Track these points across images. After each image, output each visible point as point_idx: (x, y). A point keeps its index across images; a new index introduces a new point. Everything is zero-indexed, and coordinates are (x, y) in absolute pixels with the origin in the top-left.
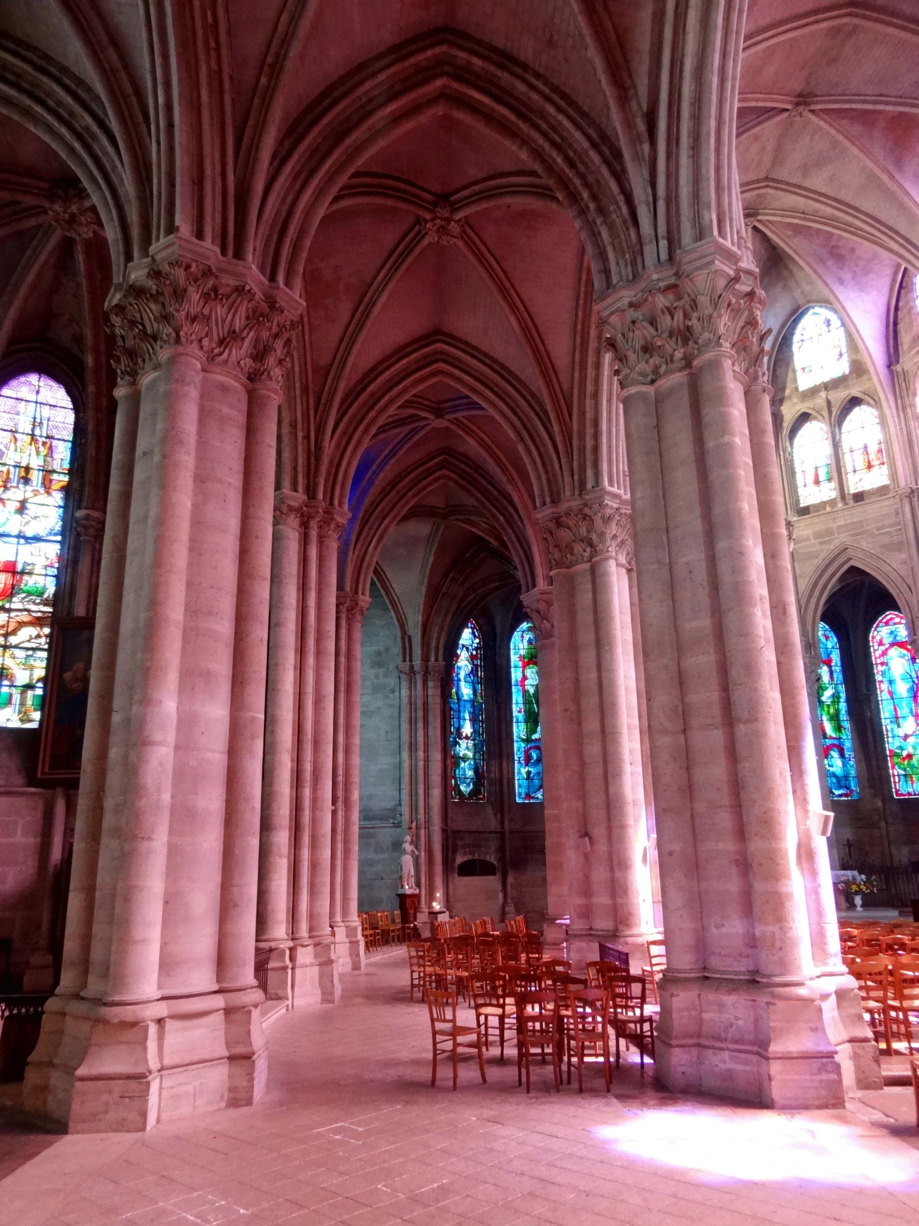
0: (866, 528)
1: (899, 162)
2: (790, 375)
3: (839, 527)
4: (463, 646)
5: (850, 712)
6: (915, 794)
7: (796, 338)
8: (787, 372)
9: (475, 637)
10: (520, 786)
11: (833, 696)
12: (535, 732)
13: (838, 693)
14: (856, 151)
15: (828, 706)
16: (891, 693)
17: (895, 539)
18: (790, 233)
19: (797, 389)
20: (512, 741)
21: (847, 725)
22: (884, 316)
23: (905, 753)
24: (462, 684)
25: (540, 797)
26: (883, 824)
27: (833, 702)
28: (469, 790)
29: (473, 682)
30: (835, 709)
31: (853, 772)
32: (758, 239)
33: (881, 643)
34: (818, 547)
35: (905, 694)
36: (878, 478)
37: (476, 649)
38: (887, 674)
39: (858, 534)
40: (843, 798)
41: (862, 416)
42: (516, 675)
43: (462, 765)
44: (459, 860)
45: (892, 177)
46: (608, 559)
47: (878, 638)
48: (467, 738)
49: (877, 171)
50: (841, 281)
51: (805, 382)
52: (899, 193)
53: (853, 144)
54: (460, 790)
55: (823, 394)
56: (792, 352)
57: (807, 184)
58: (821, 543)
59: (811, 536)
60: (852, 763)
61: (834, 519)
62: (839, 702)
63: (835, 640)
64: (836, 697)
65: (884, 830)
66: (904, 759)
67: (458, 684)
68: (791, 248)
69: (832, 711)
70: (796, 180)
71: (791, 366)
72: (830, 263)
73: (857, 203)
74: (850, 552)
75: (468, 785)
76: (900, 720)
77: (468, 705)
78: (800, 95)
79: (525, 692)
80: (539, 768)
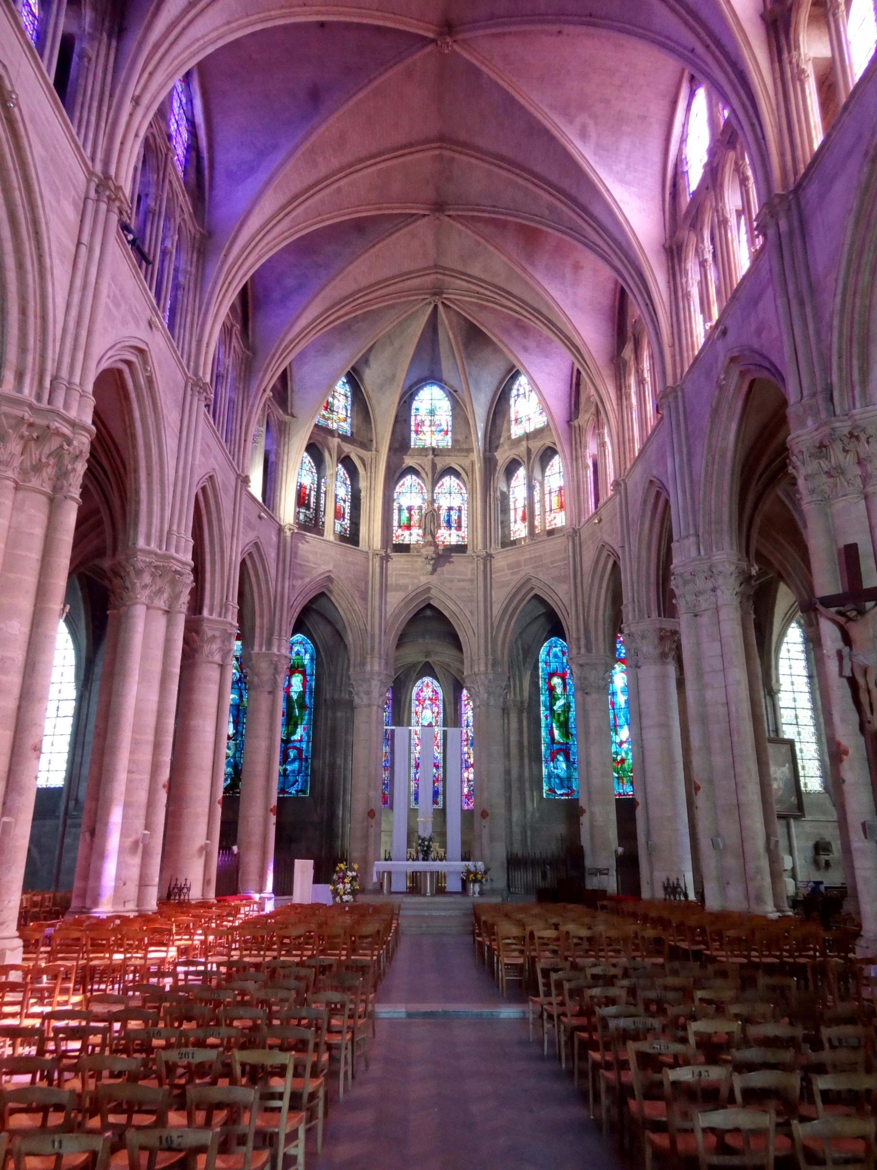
1: (530, 258)
3: (525, 560)
7: (514, 392)
8: (503, 422)
11: (564, 705)
12: (294, 733)
13: (569, 703)
14: (491, 248)
15: (559, 715)
17: (563, 573)
18: (475, 308)
19: (509, 437)
22: (569, 379)
23: (619, 758)
25: (293, 792)
27: (564, 711)
30: (565, 717)
35: (623, 705)
36: (559, 520)
41: (556, 462)
42: (282, 683)
45: (525, 270)
46: (137, 603)
49: (511, 265)
50: (525, 349)
51: (516, 431)
52: (531, 281)
53: (488, 241)
55: (524, 443)
56: (509, 406)
57: (469, 272)
58: (512, 574)
61: (523, 552)
62: (569, 711)
64: (567, 707)
66: (618, 763)
68: (477, 320)
69: (562, 718)
70: (459, 267)
72: (516, 333)
73: (508, 288)
76: (618, 729)
78: (436, 203)
79: (288, 698)
80: (296, 765)
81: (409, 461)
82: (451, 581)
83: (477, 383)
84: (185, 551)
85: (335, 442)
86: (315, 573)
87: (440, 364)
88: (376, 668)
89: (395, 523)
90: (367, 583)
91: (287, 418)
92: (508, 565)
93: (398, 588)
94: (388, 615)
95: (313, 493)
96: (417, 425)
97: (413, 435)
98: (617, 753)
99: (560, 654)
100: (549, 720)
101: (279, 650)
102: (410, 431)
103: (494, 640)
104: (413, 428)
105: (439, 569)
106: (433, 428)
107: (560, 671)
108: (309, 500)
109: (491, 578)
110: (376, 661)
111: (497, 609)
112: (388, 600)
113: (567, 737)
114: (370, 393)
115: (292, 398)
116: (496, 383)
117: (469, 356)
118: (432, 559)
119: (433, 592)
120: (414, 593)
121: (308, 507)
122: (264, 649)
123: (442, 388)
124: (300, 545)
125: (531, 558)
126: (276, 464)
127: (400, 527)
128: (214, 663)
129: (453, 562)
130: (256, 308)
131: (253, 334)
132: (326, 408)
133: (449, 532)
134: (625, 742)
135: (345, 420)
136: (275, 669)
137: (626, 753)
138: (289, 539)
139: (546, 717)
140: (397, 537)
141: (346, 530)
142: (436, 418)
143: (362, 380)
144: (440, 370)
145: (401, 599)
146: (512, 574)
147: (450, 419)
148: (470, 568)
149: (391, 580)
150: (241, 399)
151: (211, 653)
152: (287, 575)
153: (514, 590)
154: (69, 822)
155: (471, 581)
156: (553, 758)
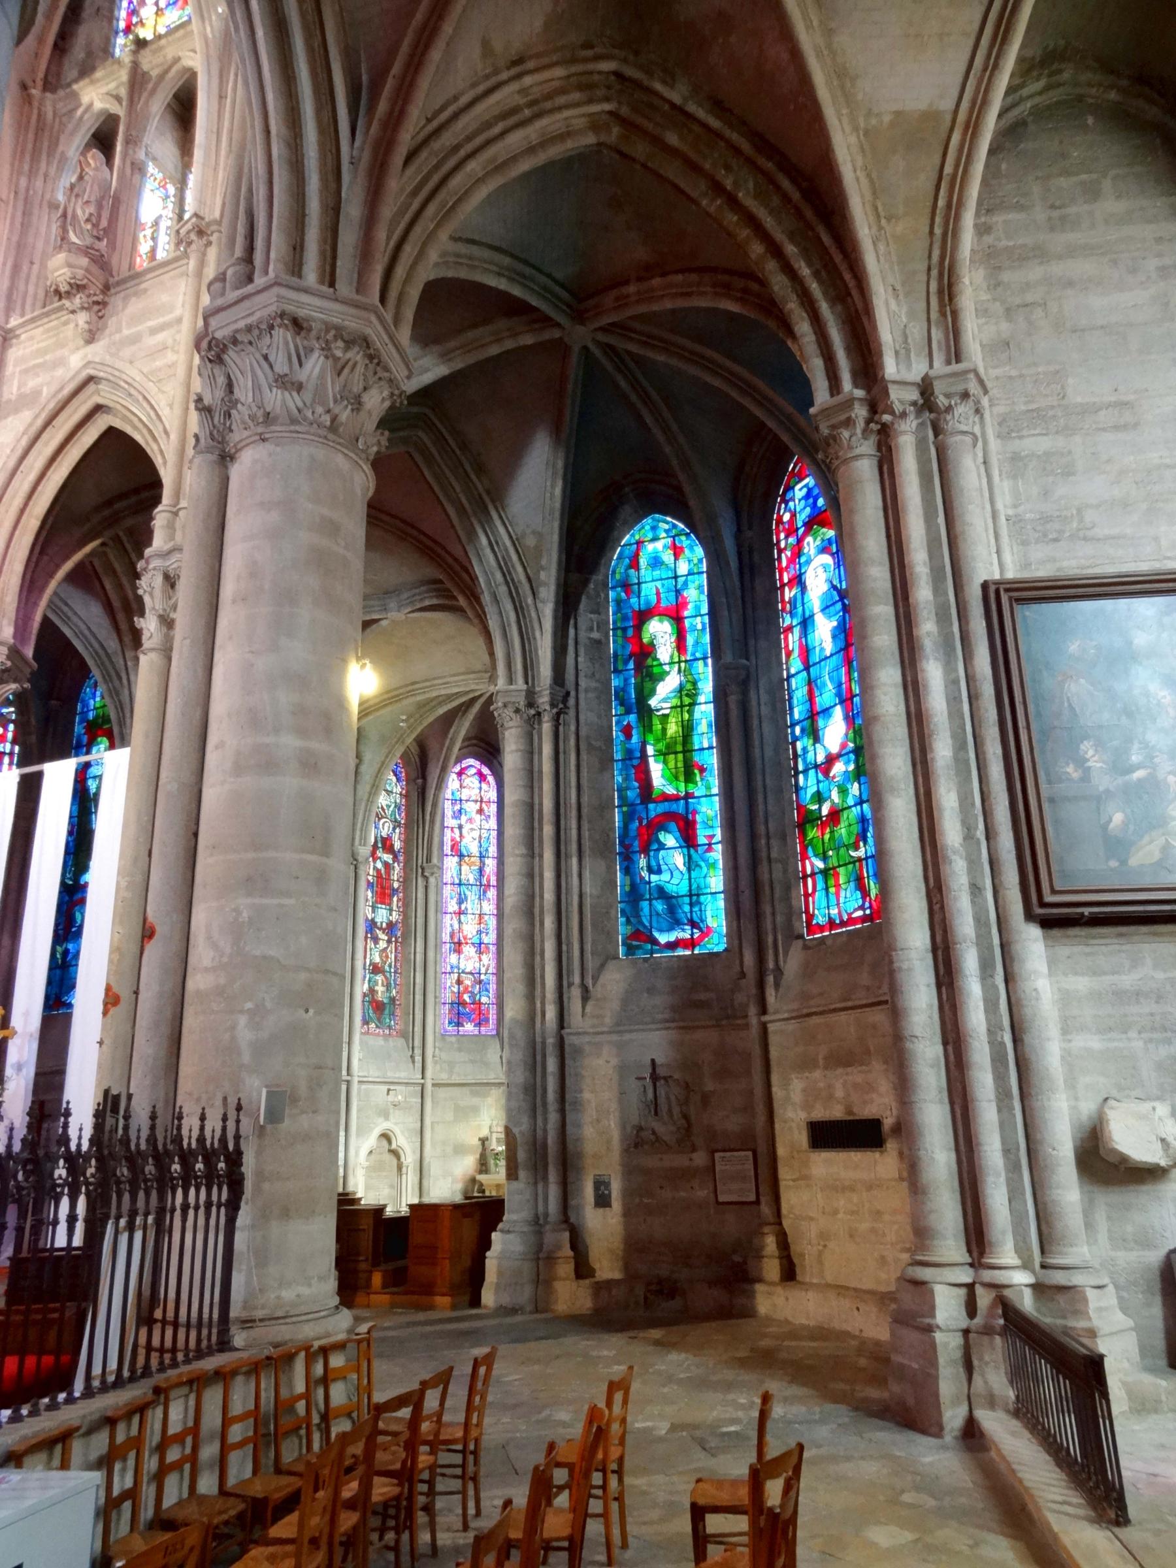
5: (722, 724)
6: (843, 924)
11: (681, 688)
13: (695, 683)
16: (805, 652)
21: (711, 760)
23: (825, 811)
26: (753, 1010)
31: (716, 881)
33: (791, 531)
35: (829, 647)
38: (800, 609)
40: (680, 952)
47: (787, 517)
60: (717, 854)
62: (693, 704)
63: (699, 552)
64: (687, 695)
65: (754, 1031)
69: (673, 729)
76: (821, 723)
98: (819, 798)
99: (668, 557)
100: (635, 739)
105: (112, 322)
107: (668, 600)
113: (689, 777)
129: (145, 290)
134: (839, 756)
137: (843, 791)
139: (627, 731)
145: (22, 429)
156: (648, 842)
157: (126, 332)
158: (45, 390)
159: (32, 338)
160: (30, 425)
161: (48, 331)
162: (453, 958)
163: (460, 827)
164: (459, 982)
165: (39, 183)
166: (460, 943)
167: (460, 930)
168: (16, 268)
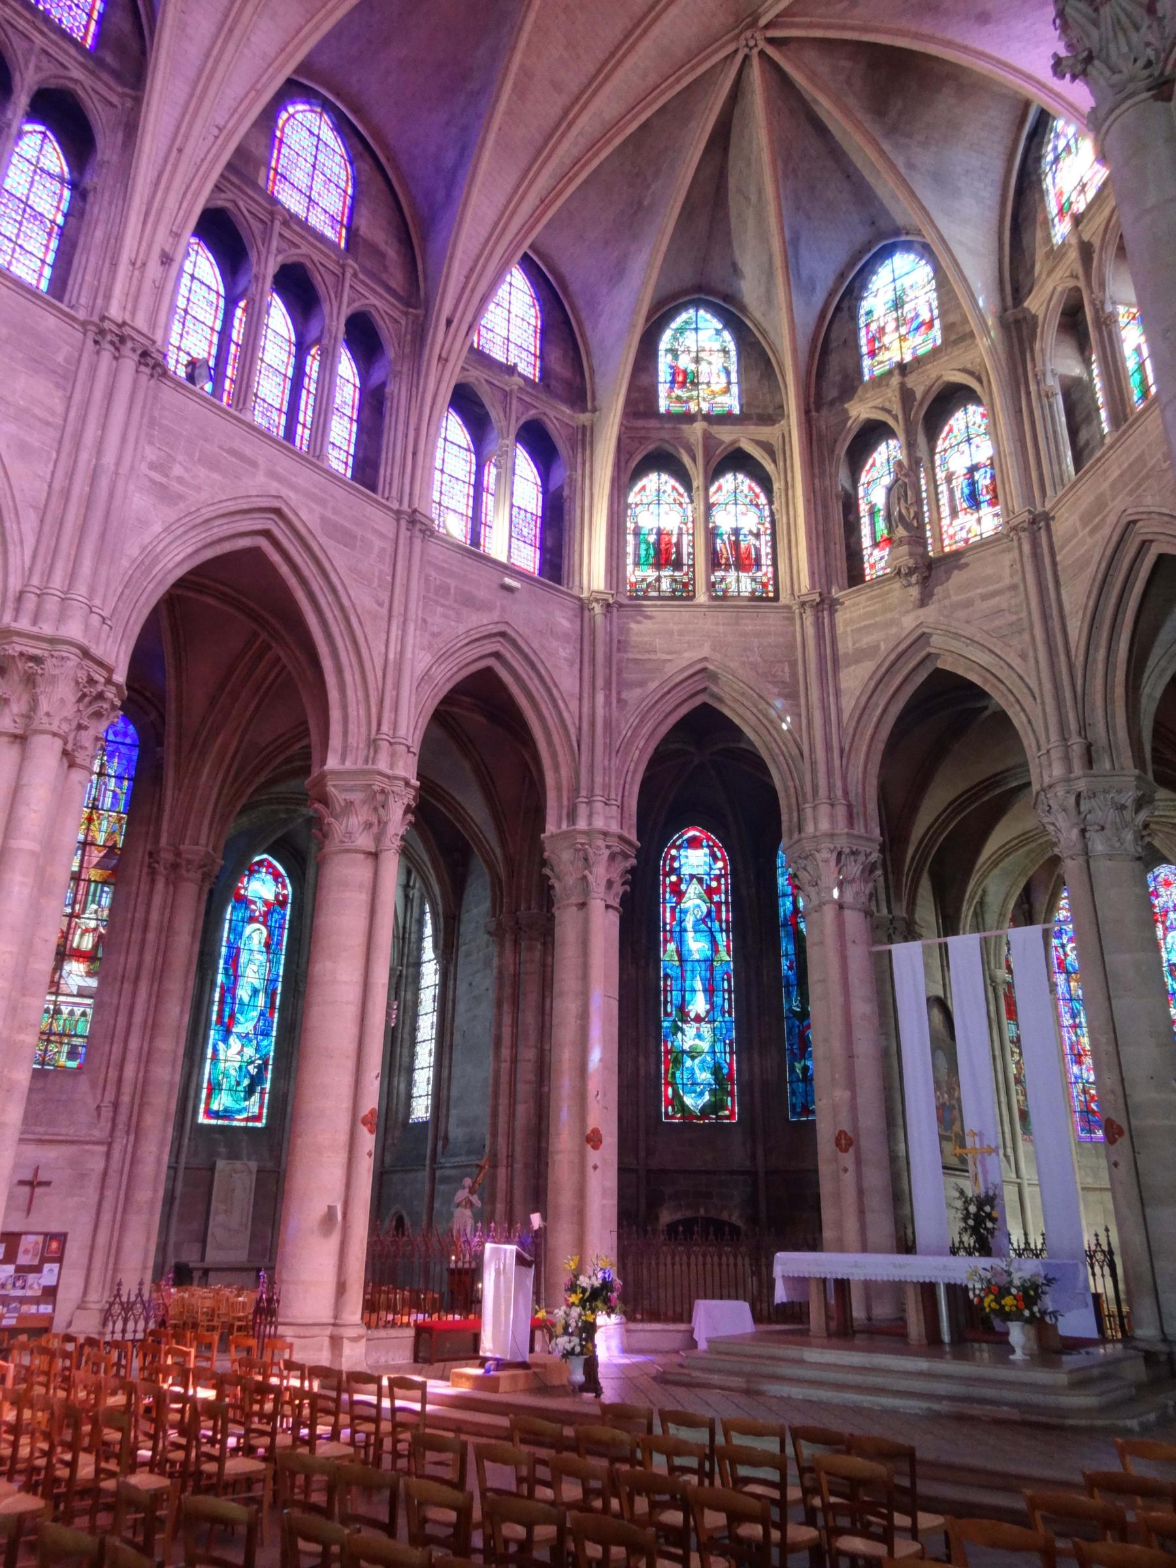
0: (1150, 465)
2: (1039, 234)
3: (1113, 485)
4: (692, 876)
8: (1034, 234)
9: (715, 859)
10: (793, 1093)
20: (780, 1019)
24: (690, 936)
28: (701, 1102)
29: (711, 931)
32: (810, 55)
34: (1090, 541)
37: (717, 878)
39: (1139, 485)
43: (688, 1063)
44: (666, 1217)
48: (698, 1019)
54: (682, 1104)
58: (1092, 532)
59: (1078, 525)
61: (1105, 472)
67: (681, 936)
68: (853, 28)
71: (1040, 217)
74: (1144, 529)
75: (701, 1094)
77: (700, 970)
81: (860, 411)
82: (968, 604)
83: (940, 179)
84: (62, 618)
85: (699, 426)
86: (670, 669)
87: (876, 196)
88: (824, 826)
89: (866, 542)
90: (793, 665)
91: (584, 418)
92: (1081, 519)
93: (861, 655)
94: (846, 716)
95: (686, 539)
96: (872, 341)
97: (867, 362)
101: (590, 824)
102: (860, 357)
103: (1081, 701)
104: (864, 350)
105: (938, 590)
106: (903, 330)
108: (679, 553)
109: (1054, 564)
110: (824, 809)
111: (1076, 627)
112: (843, 685)
114: (765, 325)
115: (593, 383)
116: (998, 165)
117: (892, 131)
118: (911, 572)
119: (937, 641)
120: (893, 657)
121: (678, 565)
122: (564, 826)
123: (908, 247)
124: (633, 626)
125: (1121, 475)
126: (572, 499)
127: (876, 545)
128: (356, 851)
129: (967, 565)
130: (424, 239)
131: (426, 278)
132: (683, 384)
133: (976, 516)
135: (727, 391)
136: (586, 859)
138: (599, 619)
140: (872, 566)
141: (765, 585)
142: (907, 308)
143: (743, 308)
144: (887, 213)
146: (1092, 532)
147: (935, 295)
148: (1007, 564)
149: (846, 645)
150: (404, 389)
151: (349, 834)
152: (600, 682)
153: (1104, 565)
154: (438, 1173)
155: (1014, 587)
157: (955, 598)
158: (882, 645)
159: (854, 605)
160: (875, 672)
161: (872, 598)
162: (1075, 1069)
163: (1063, 946)
164: (1085, 1091)
165: (828, 482)
166: (1080, 1055)
167: (1078, 1042)
168: (826, 551)
